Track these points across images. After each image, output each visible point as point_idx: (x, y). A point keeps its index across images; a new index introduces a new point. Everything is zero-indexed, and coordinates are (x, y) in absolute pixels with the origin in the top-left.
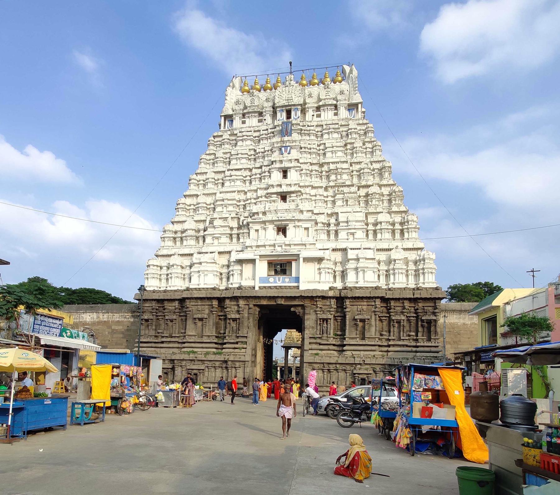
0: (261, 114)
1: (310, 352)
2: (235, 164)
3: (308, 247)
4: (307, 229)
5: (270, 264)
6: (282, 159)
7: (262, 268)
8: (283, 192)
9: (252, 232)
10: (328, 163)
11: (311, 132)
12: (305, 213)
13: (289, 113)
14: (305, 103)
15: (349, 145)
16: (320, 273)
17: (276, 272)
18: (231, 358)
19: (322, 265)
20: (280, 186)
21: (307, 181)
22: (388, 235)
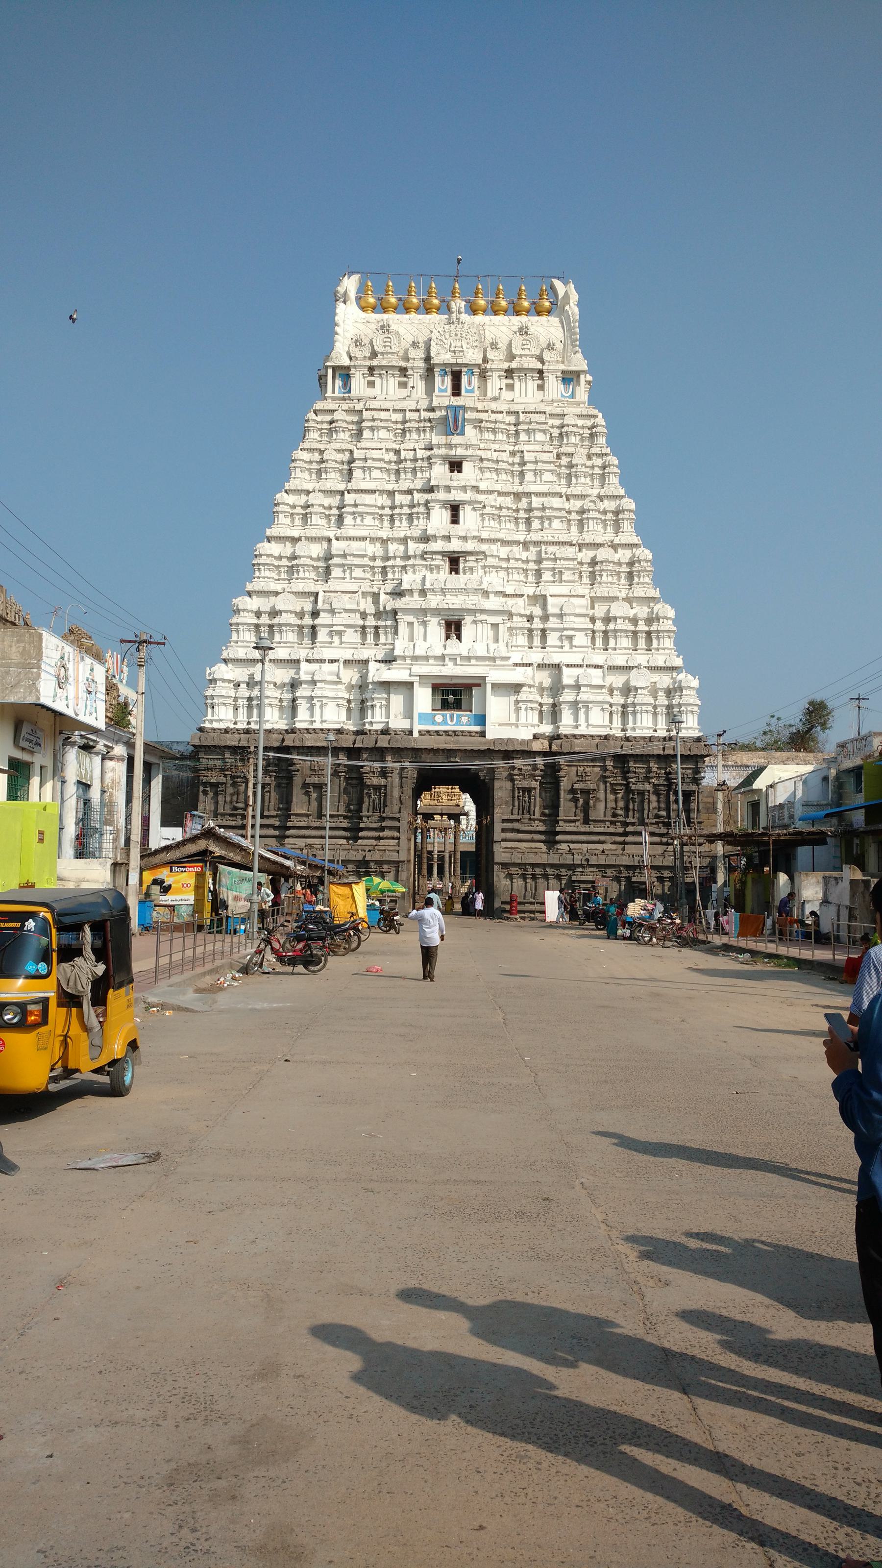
0: (403, 371)
1: (504, 844)
2: (360, 480)
3: (498, 662)
4: (495, 626)
5: (435, 688)
6: (449, 483)
7: (424, 699)
8: (454, 552)
9: (403, 628)
10: (529, 495)
11: (498, 425)
12: (491, 596)
13: (456, 377)
14: (485, 360)
15: (563, 458)
16: (518, 709)
17: (445, 705)
18: (377, 856)
19: (523, 696)
20: (448, 538)
21: (491, 529)
22: (625, 642)
